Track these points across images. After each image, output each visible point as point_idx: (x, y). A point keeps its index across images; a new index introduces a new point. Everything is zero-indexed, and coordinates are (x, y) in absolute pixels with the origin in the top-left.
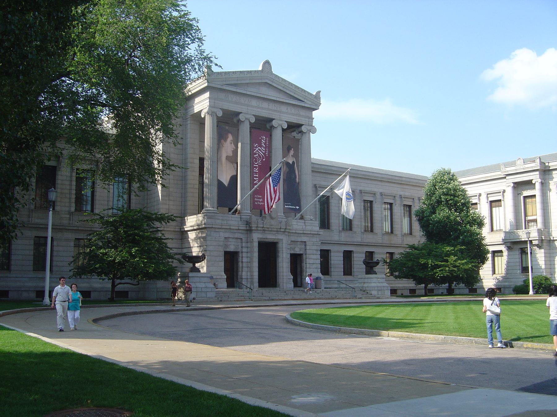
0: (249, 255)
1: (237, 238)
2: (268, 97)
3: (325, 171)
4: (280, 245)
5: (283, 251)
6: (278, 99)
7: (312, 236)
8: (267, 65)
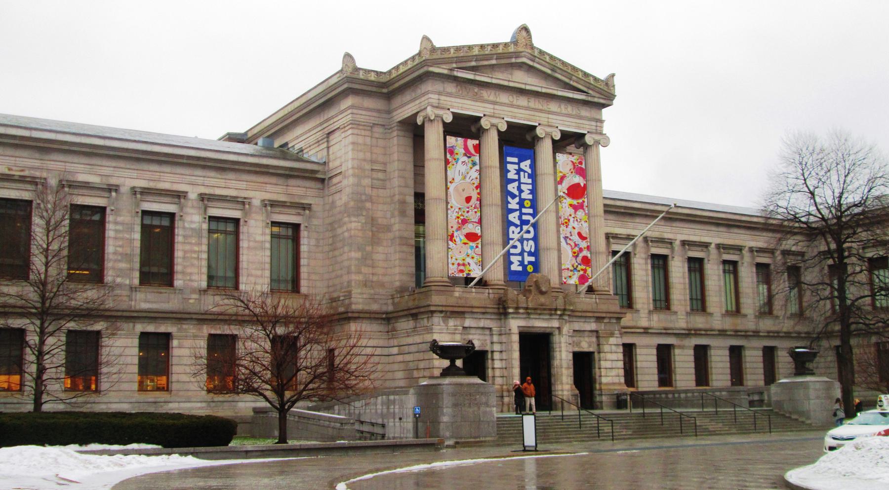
0: (504, 356)
1: (483, 328)
2: (528, 87)
4: (556, 338)
5: (560, 347)
8: (524, 33)
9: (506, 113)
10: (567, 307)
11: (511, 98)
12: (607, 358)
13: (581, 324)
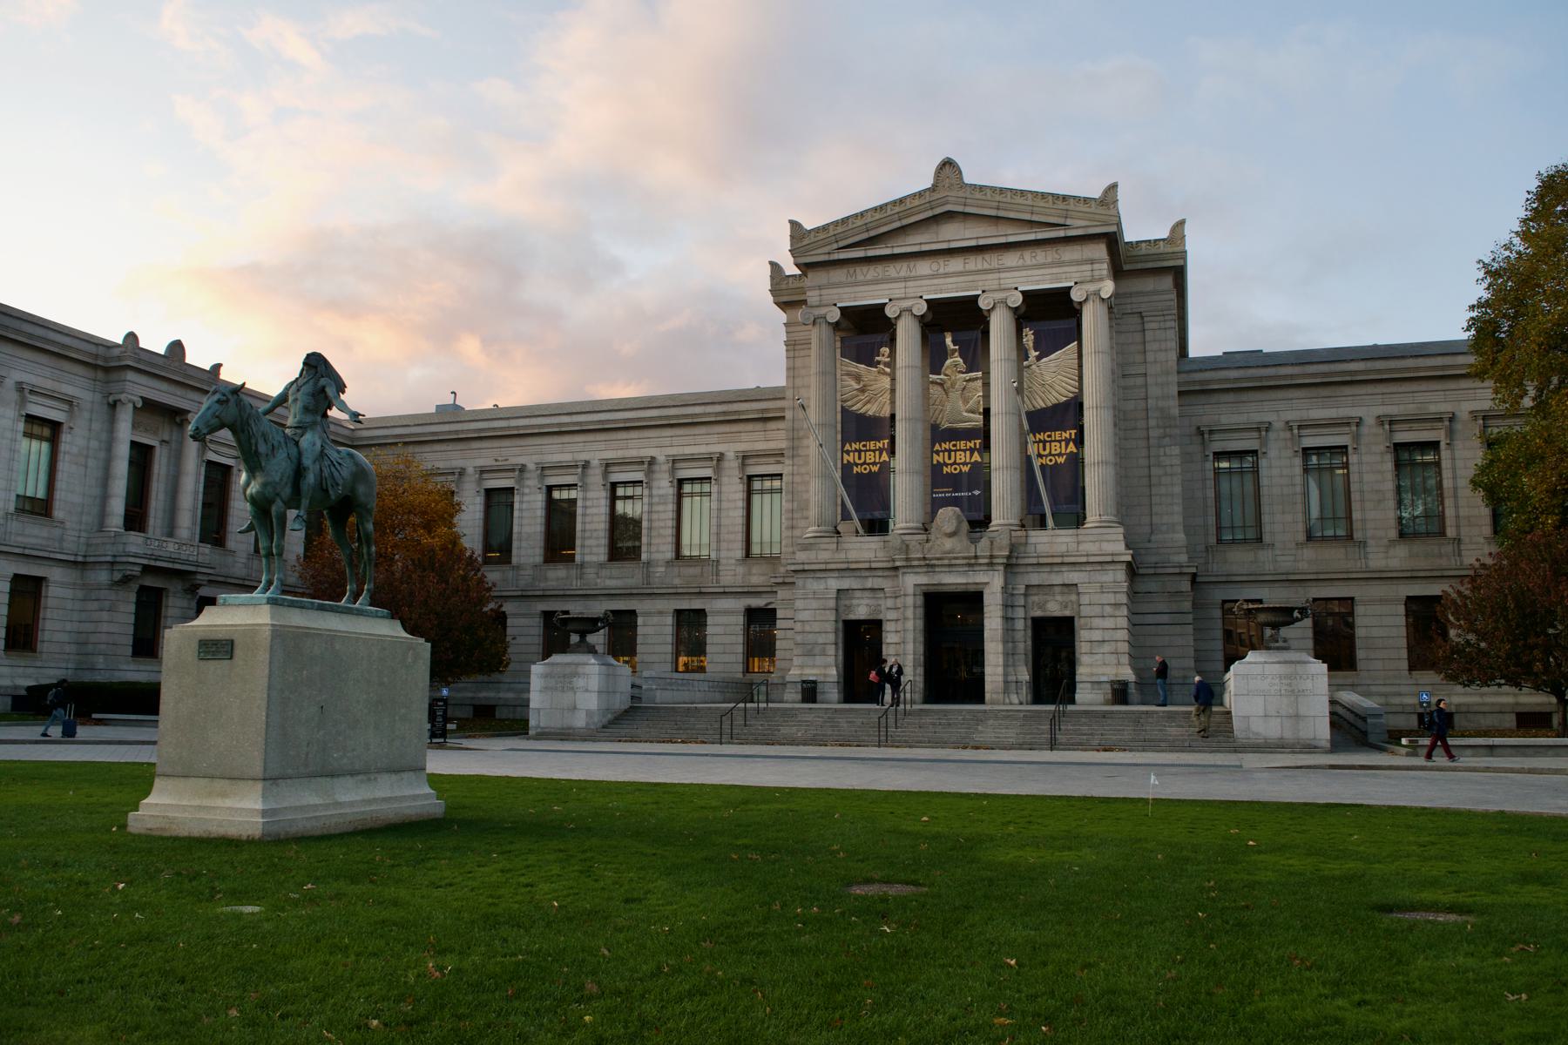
2: (954, 245)
6: (982, 242)
7: (1099, 568)
9: (925, 288)
10: (995, 553)
11: (935, 266)
12: (1094, 625)
13: (1045, 576)
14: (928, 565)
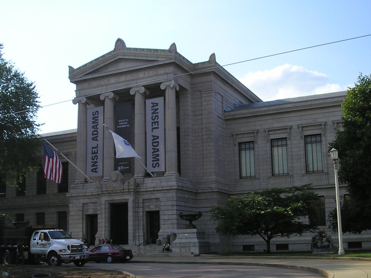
3: (275, 112)
10: (130, 188)
11: (116, 79)
14: (108, 193)
